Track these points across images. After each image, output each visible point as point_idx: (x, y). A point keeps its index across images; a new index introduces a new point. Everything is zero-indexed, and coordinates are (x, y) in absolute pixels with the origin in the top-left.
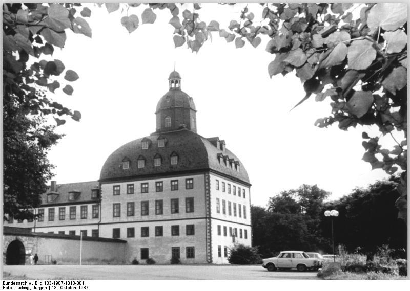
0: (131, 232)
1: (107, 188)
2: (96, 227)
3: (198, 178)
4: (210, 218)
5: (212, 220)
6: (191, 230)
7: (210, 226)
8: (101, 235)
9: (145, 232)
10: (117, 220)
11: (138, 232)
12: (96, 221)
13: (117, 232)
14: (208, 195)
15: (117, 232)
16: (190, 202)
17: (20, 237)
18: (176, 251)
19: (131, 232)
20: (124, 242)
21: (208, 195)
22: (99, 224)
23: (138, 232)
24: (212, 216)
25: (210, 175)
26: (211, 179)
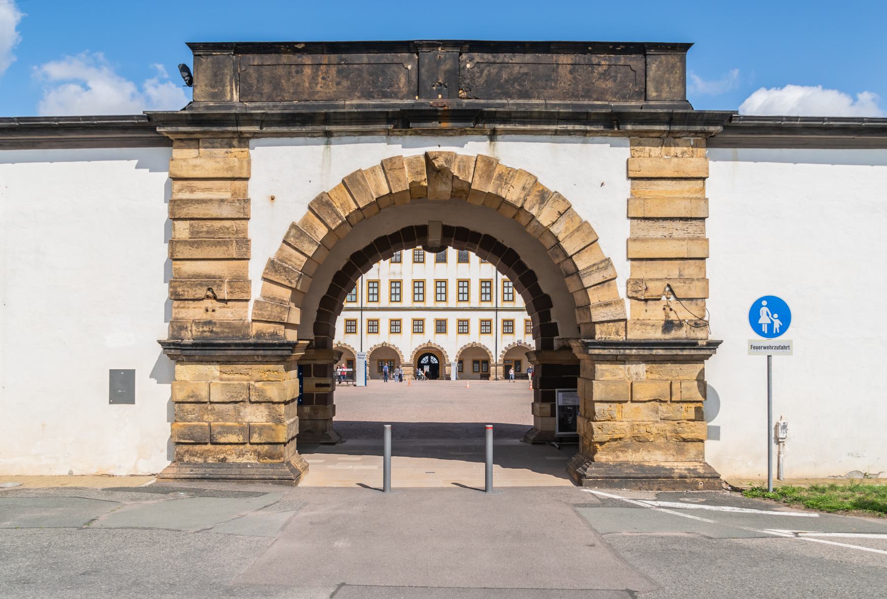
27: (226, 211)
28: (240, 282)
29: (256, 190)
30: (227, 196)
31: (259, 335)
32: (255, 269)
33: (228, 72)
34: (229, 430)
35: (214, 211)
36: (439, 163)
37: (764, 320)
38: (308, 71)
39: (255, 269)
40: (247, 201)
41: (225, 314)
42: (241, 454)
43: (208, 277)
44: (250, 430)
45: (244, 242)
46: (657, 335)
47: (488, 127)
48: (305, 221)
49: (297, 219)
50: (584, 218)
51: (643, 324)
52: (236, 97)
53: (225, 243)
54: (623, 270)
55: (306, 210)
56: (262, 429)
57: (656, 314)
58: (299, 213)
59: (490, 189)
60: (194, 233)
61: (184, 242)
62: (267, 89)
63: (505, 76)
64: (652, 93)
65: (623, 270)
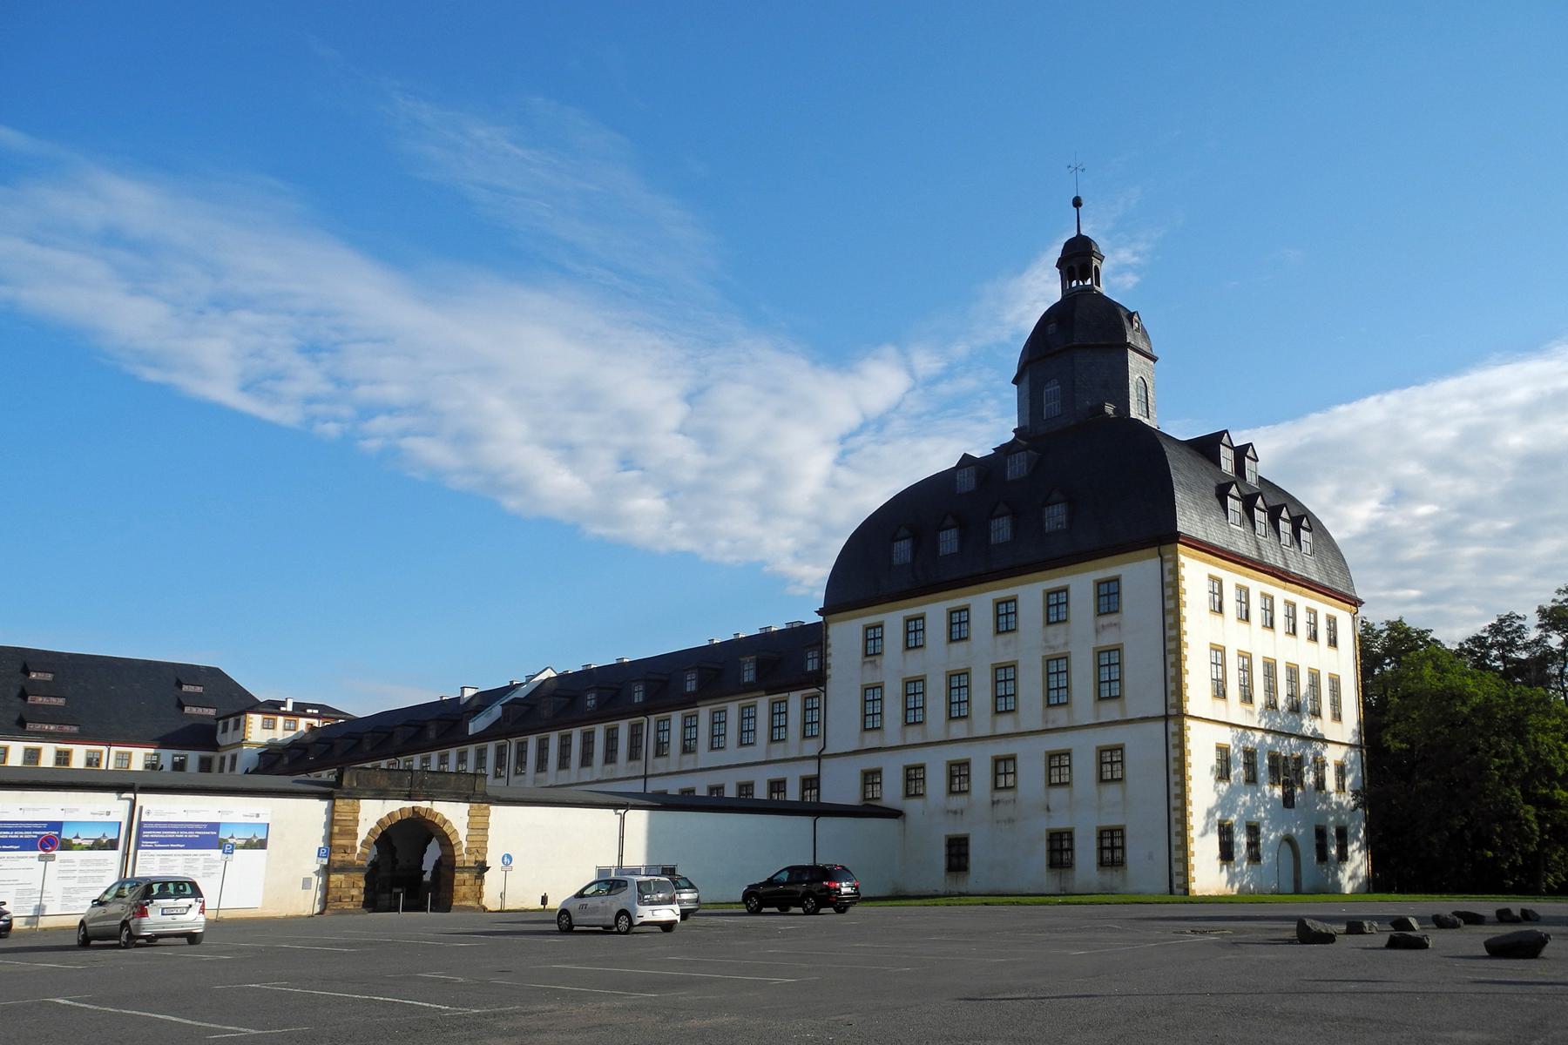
0: (914, 777)
1: (846, 635)
2: (810, 769)
3: (1136, 573)
4: (1181, 715)
5: (1188, 722)
6: (1110, 762)
7: (1181, 745)
8: (829, 795)
9: (958, 772)
10: (872, 740)
11: (936, 780)
12: (811, 748)
13: (871, 777)
14: (1173, 633)
15: (871, 777)
16: (1109, 660)
17: (425, 804)
18: (1059, 847)
19: (914, 777)
20: (895, 814)
21: (1173, 633)
22: (819, 757)
23: (936, 780)
24: (1191, 707)
25: (1182, 558)
26: (1183, 572)
27: (351, 824)
28: (354, 848)
29: (361, 816)
30: (351, 818)
31: (358, 865)
32: (359, 843)
33: (354, 778)
34: (346, 897)
35: (348, 823)
36: (416, 810)
37: (505, 861)
38: (379, 778)
39: (359, 843)
40: (358, 821)
41: (348, 858)
42: (349, 905)
43: (344, 846)
44: (353, 897)
45: (356, 835)
46: (473, 865)
47: (430, 798)
48: (376, 827)
49: (373, 827)
50: (455, 828)
51: (469, 861)
52: (355, 784)
53: (351, 834)
54: (465, 844)
55: (375, 824)
56: (357, 897)
57: (473, 858)
58: (373, 825)
59: (430, 819)
60: (340, 830)
61: (337, 834)
62: (366, 783)
63: (436, 782)
64: (476, 789)
65: (465, 844)
